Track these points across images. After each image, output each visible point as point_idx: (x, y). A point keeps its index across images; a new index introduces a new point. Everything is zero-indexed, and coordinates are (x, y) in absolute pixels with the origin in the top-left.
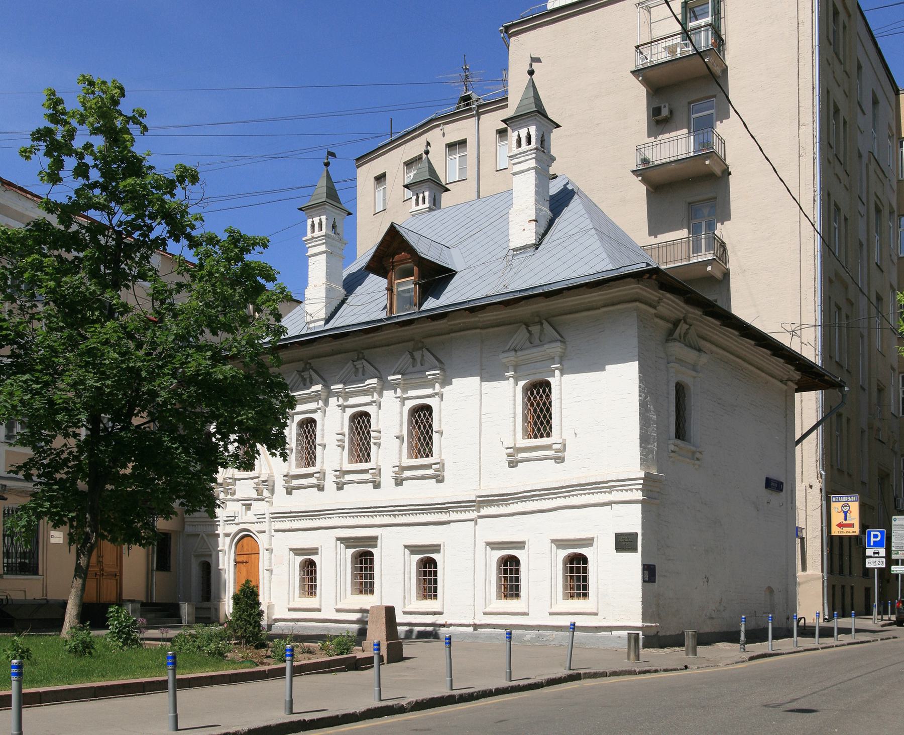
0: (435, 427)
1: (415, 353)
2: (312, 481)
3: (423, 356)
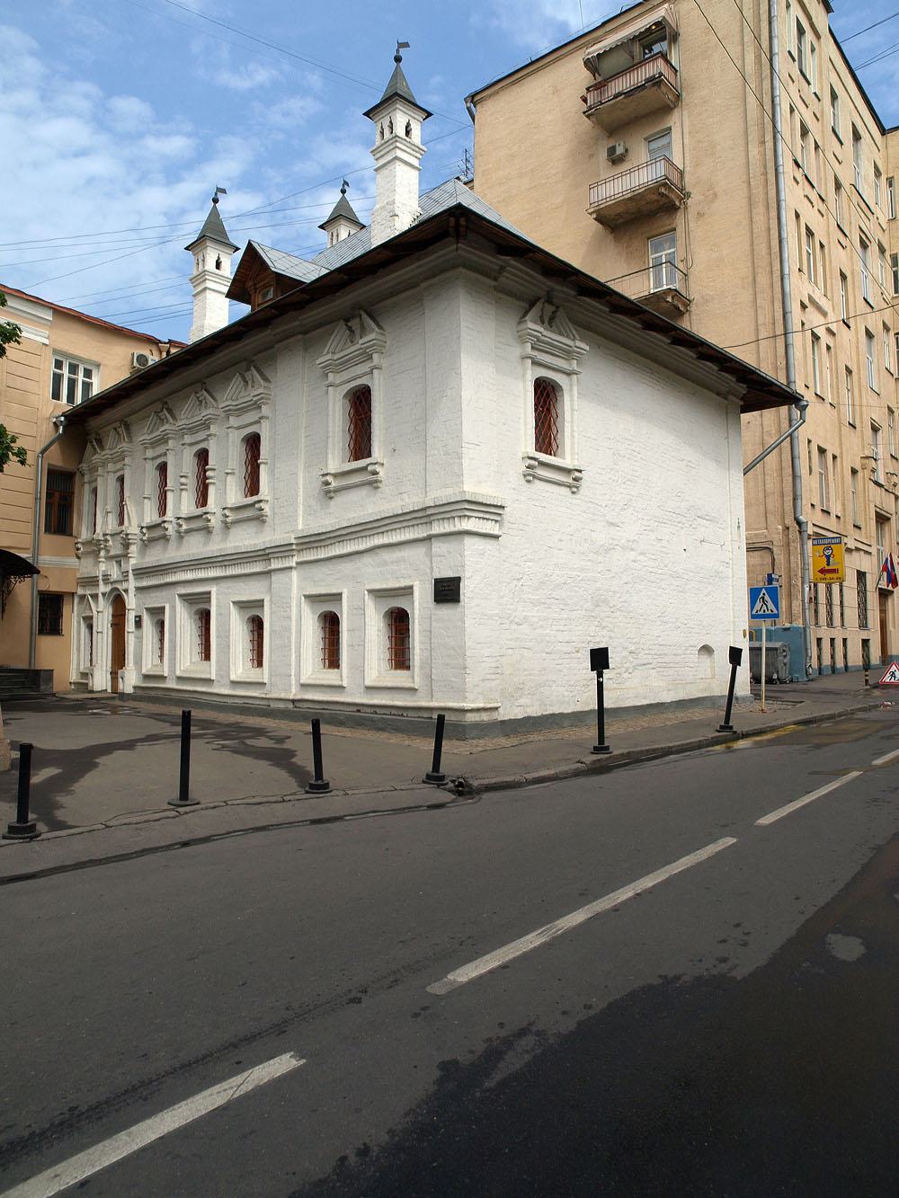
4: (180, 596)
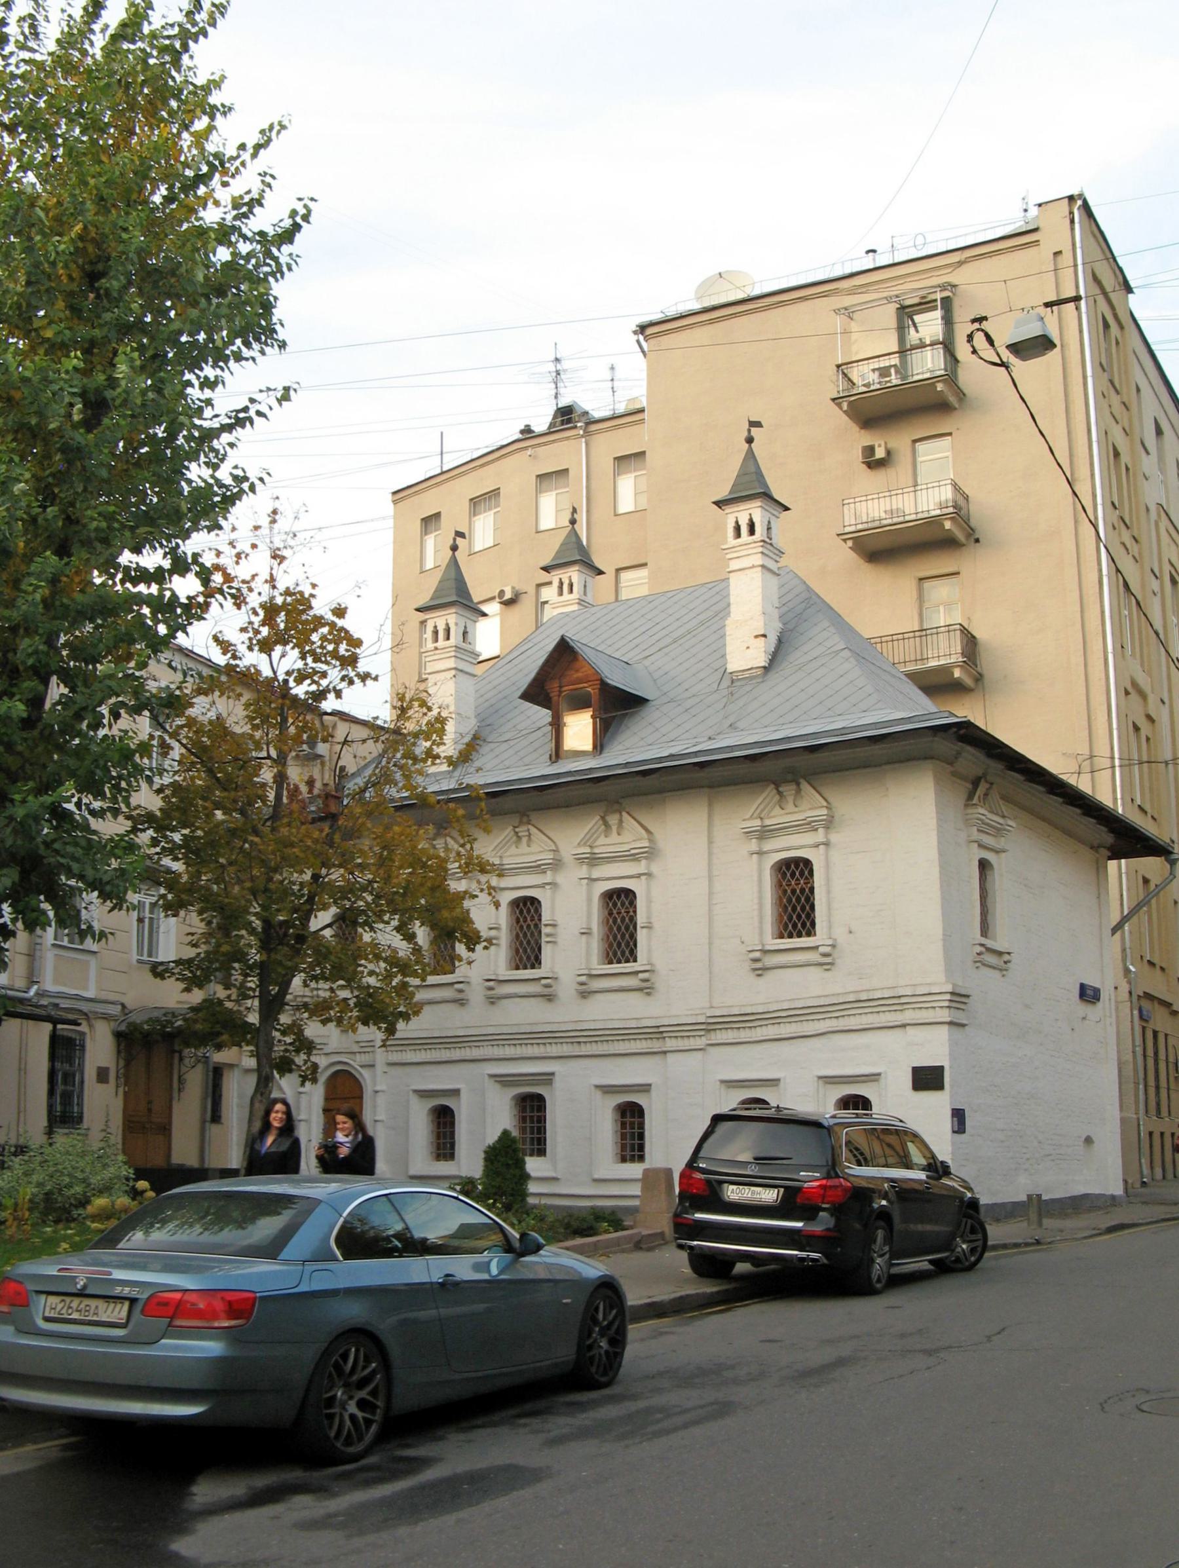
0: (641, 919)
3: (621, 821)
4: (491, 1076)
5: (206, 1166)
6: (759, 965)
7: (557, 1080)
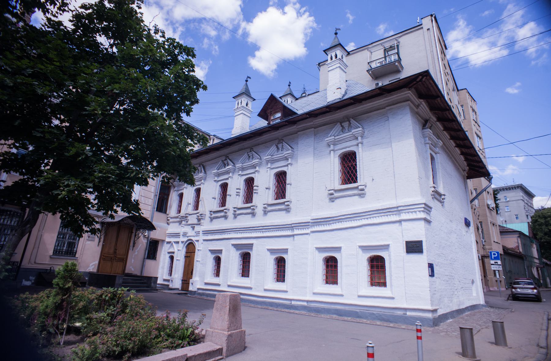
1: (278, 145)
2: (222, 214)
5: (145, 274)
6: (332, 196)
7: (254, 248)
